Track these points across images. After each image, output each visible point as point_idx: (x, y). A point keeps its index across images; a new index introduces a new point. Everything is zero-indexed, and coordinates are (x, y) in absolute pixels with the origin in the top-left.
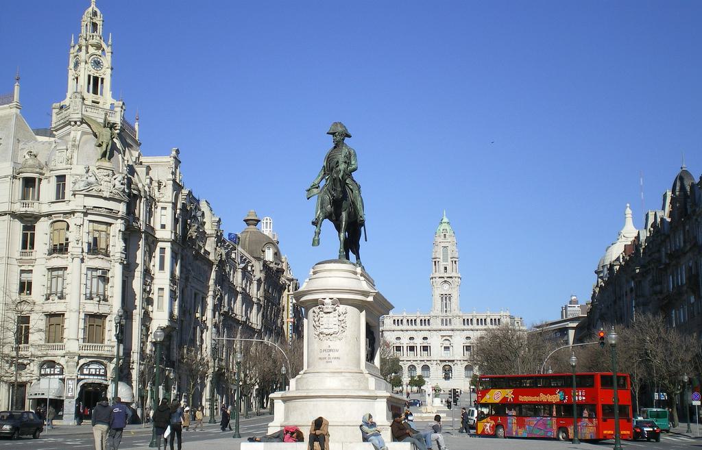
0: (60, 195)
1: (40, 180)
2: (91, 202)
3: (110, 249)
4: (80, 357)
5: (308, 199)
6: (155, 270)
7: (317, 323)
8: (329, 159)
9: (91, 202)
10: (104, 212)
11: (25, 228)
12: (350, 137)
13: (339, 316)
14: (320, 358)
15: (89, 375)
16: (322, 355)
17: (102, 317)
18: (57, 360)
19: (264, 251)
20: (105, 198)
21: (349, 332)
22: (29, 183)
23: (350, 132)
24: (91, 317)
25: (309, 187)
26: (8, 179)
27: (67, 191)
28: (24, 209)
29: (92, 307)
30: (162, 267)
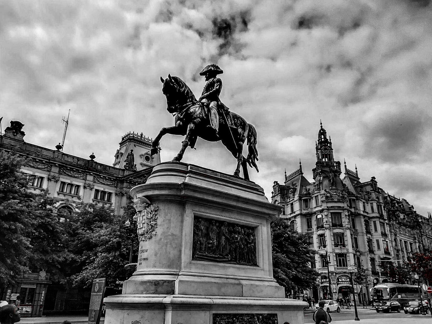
1: (310, 199)
2: (330, 205)
3: (343, 223)
4: (336, 274)
6: (373, 231)
9: (330, 205)
11: (307, 220)
15: (342, 281)
20: (336, 202)
21: (159, 231)
22: (306, 201)
26: (298, 201)
27: (320, 202)
28: (305, 212)
29: (338, 251)
30: (376, 230)
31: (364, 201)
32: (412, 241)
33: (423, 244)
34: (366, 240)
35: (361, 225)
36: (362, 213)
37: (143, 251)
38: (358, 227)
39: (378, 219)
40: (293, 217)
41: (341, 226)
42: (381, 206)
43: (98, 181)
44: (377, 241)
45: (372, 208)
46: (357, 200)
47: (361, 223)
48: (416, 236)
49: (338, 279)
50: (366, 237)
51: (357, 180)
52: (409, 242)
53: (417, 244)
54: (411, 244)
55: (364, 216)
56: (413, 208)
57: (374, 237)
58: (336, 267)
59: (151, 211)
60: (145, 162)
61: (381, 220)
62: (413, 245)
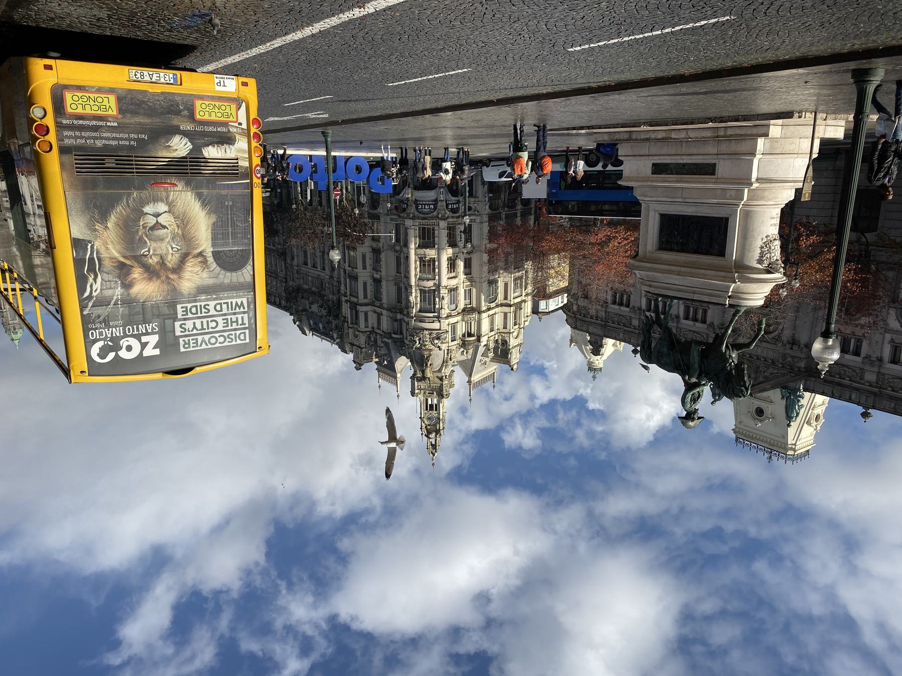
0: (454, 326)
2: (436, 325)
4: (437, 217)
6: (370, 282)
9: (436, 325)
10: (427, 320)
17: (420, 246)
18: (451, 214)
24: (431, 245)
30: (365, 284)
31: (378, 331)
33: (285, 263)
34: (383, 270)
35: (388, 293)
36: (384, 312)
37: (775, 225)
38: (393, 289)
39: (360, 302)
40: (493, 308)
41: (423, 292)
42: (352, 323)
43: (854, 371)
44: (364, 268)
45: (366, 320)
46: (390, 334)
47: (388, 296)
49: (435, 208)
50: (383, 273)
51: (381, 368)
52: (309, 266)
53: (295, 262)
54: (306, 264)
55: (381, 307)
57: (369, 274)
58: (436, 228)
60: (763, 405)
61: (354, 299)
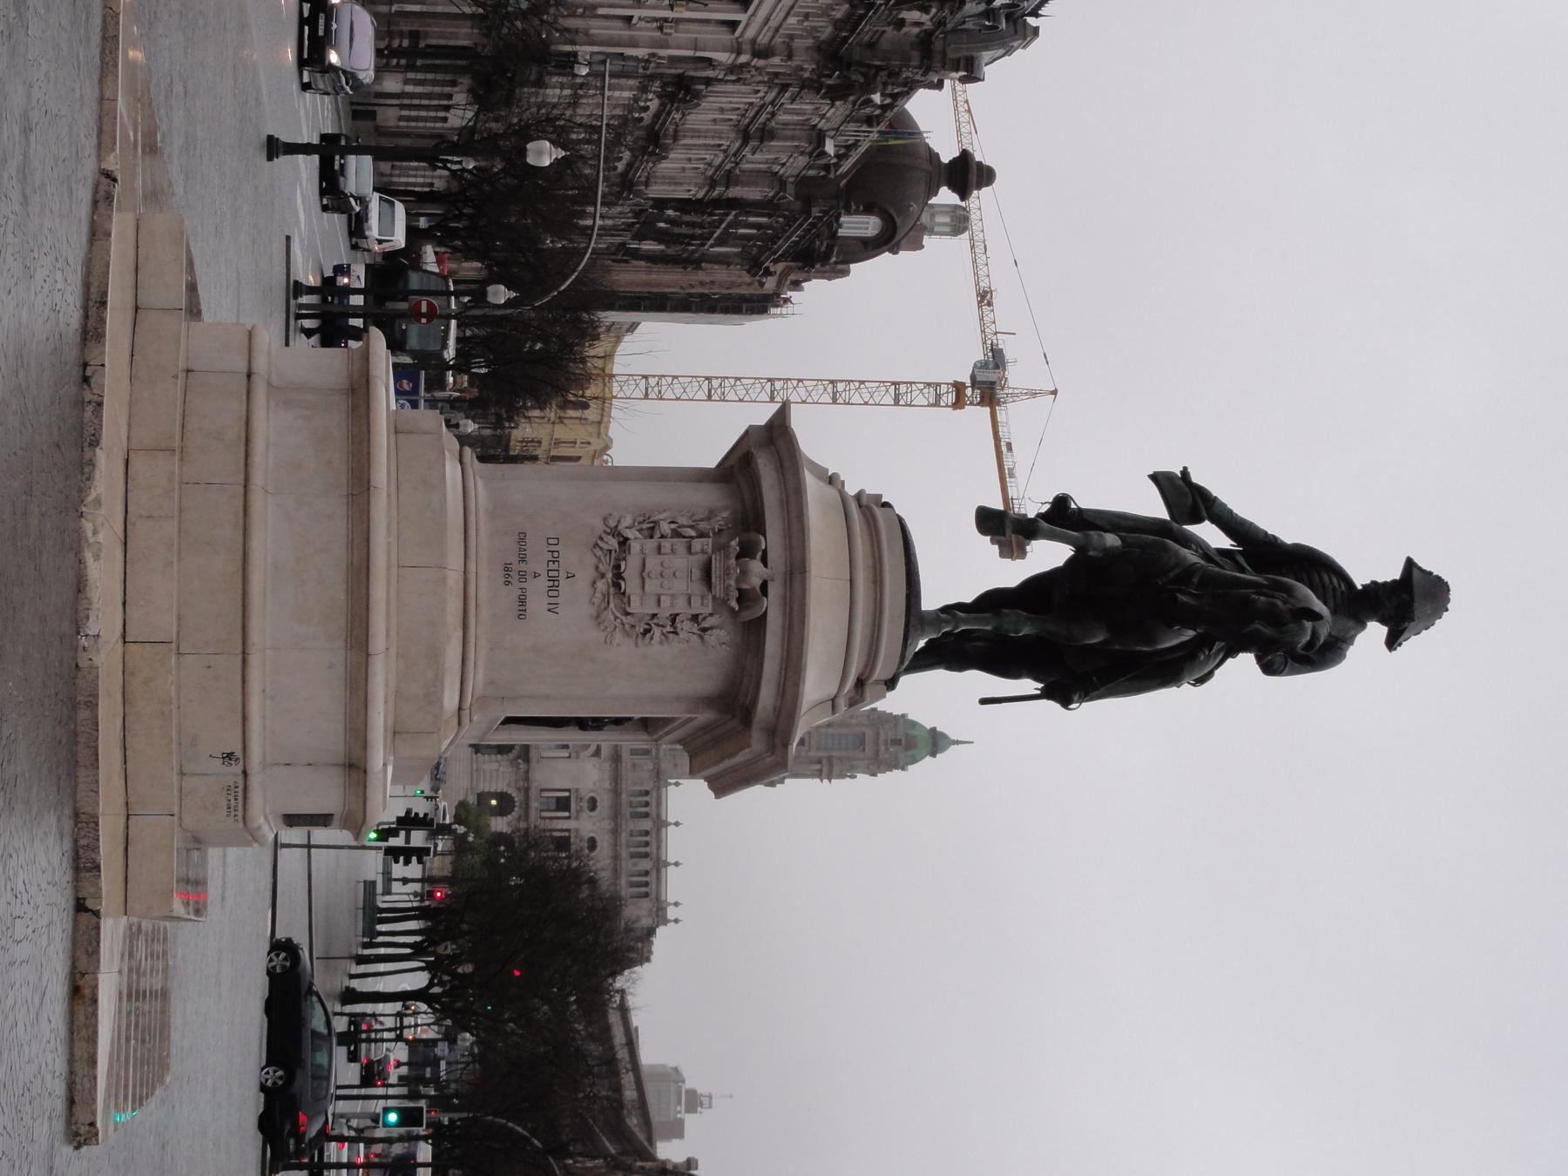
5: (1156, 478)
7: (666, 528)
8: (1311, 565)
12: (1392, 642)
13: (695, 618)
14: (522, 538)
16: (536, 545)
19: (868, 210)
21: (625, 650)
23: (1413, 645)
25: (1196, 478)
32: (750, 33)
48: (776, 60)
53: (724, 57)
54: (733, 25)
56: (963, 80)
59: (705, 630)
62: (725, 37)
